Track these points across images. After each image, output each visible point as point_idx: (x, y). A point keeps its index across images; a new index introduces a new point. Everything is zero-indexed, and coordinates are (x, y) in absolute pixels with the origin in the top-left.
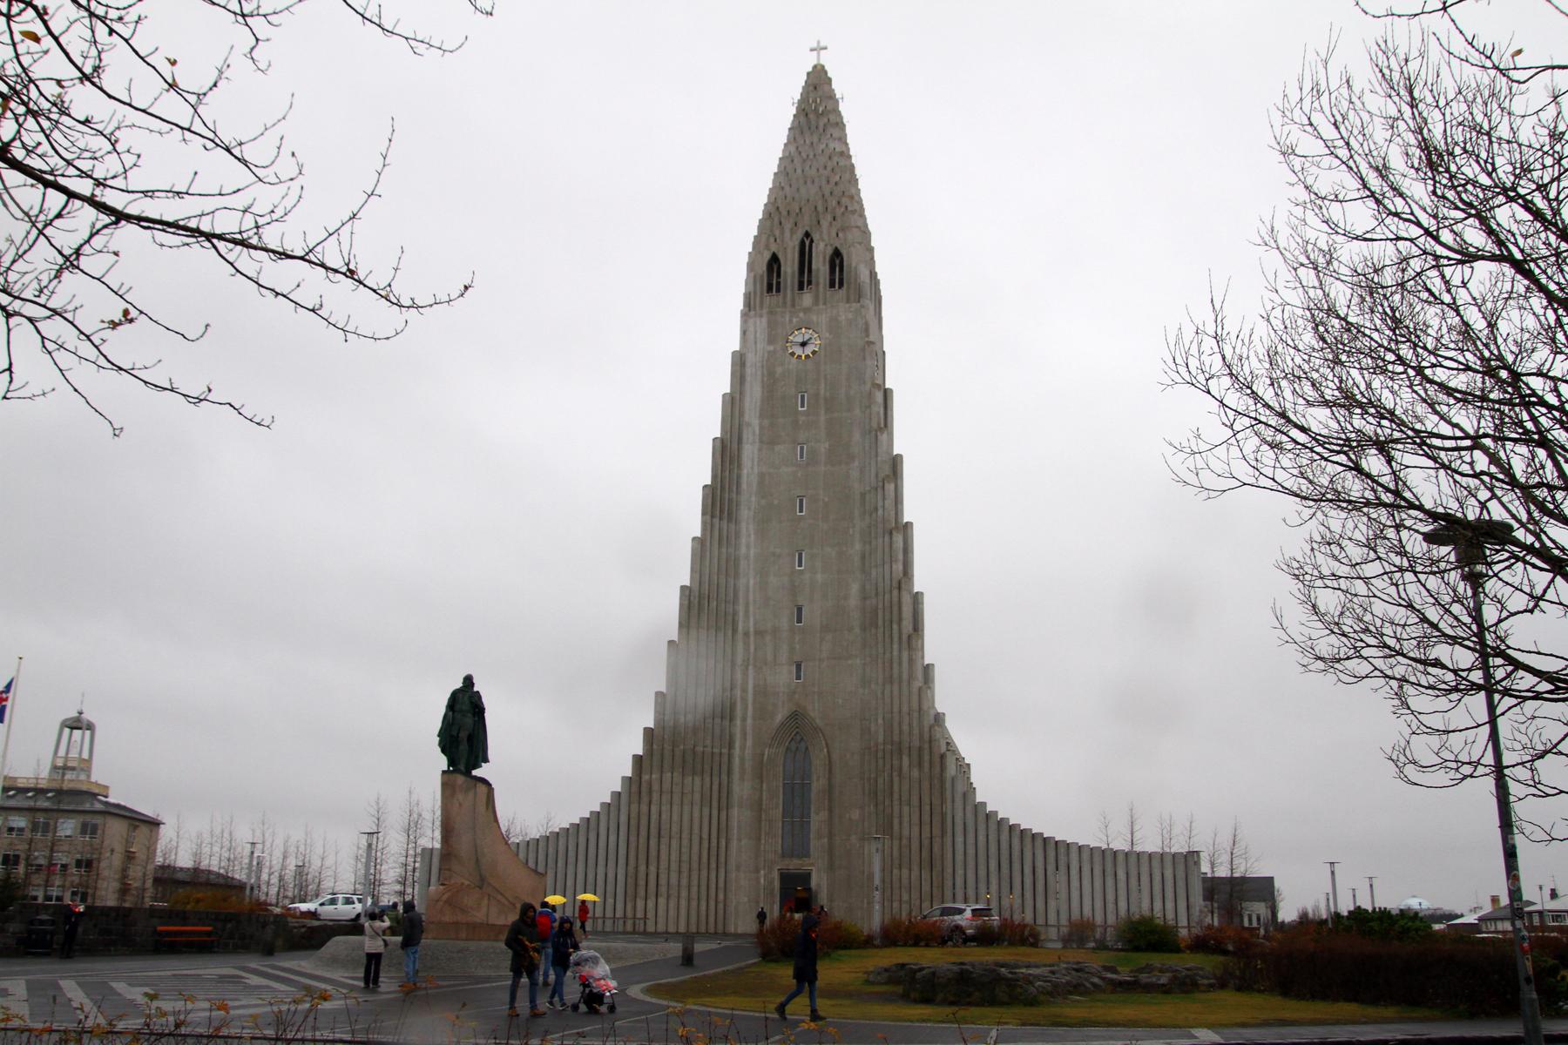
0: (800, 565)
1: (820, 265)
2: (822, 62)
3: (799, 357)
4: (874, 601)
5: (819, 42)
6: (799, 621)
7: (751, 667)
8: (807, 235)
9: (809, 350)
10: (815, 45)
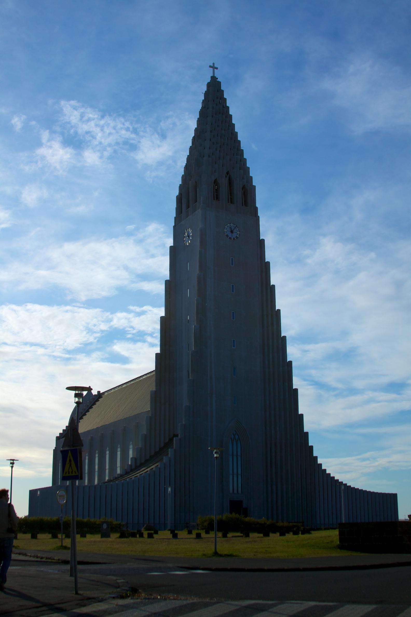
1: (238, 193)
2: (215, 76)
3: (230, 238)
5: (214, 64)
8: (228, 173)
9: (234, 235)
10: (212, 65)
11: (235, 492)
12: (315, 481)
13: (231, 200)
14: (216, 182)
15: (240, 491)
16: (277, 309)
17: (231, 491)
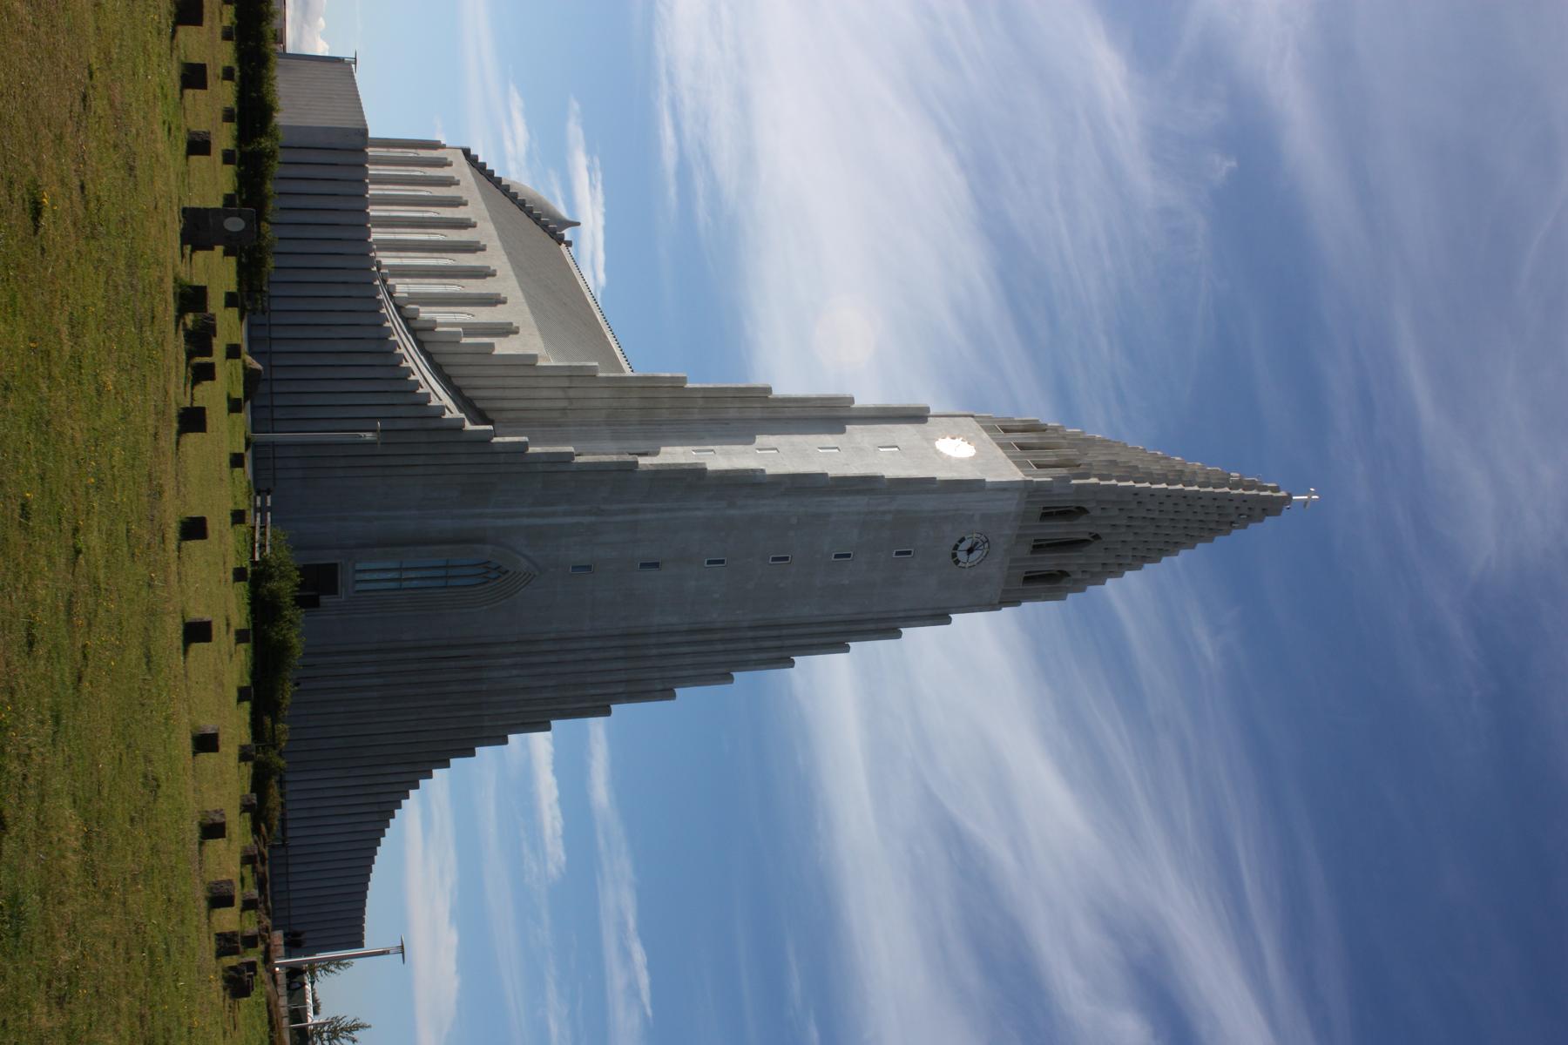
0: (709, 562)
3: (956, 547)
4: (654, 652)
6: (643, 565)
7: (593, 519)
8: (1097, 537)
9: (962, 556)
11: (359, 576)
12: (391, 764)
13: (1039, 547)
14: (1082, 511)
15: (359, 587)
16: (795, 658)
17: (358, 567)
